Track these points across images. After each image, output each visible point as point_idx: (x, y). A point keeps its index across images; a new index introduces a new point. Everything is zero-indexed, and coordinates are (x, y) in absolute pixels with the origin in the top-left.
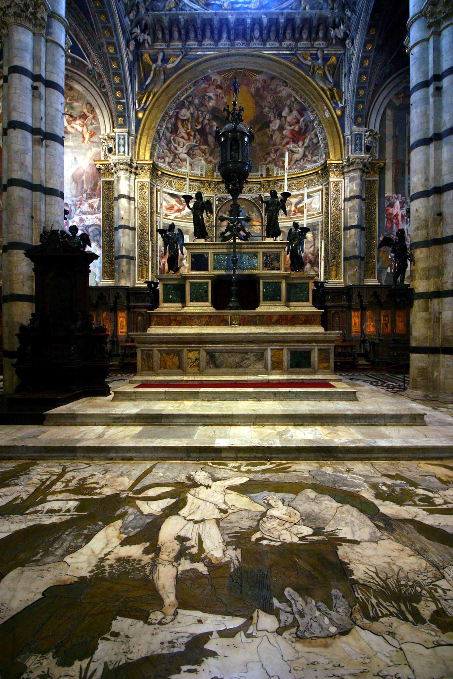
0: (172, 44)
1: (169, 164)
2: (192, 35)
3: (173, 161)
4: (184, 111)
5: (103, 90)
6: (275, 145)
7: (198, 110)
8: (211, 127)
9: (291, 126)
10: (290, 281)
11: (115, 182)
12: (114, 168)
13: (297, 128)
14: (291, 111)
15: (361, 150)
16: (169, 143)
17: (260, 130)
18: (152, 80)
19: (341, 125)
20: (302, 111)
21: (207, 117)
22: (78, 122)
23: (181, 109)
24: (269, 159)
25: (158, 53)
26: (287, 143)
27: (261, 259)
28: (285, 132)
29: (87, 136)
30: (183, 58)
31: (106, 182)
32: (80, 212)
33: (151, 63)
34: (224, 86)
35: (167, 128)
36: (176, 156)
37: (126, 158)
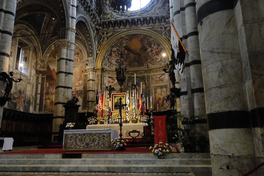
0: (109, 28)
1: (108, 66)
3: (110, 65)
4: (114, 48)
5: (85, 45)
8: (125, 52)
9: (155, 50)
11: (88, 75)
12: (88, 70)
14: (155, 45)
16: (108, 59)
17: (143, 52)
18: (102, 40)
20: (159, 45)
21: (123, 49)
22: (76, 56)
23: (113, 48)
24: (148, 62)
25: (104, 32)
28: (153, 52)
29: (79, 60)
30: (113, 32)
31: (85, 75)
32: (75, 86)
33: (102, 35)
35: (108, 55)
36: (111, 63)
37: (92, 67)
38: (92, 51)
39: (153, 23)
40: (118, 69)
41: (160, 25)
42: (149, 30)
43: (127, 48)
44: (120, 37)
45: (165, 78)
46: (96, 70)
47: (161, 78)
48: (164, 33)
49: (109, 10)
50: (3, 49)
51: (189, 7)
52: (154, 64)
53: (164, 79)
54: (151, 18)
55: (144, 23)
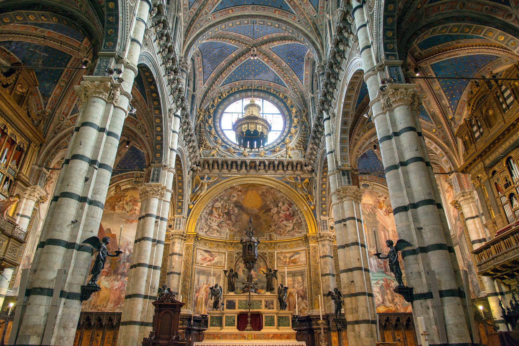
1: (206, 232)
2: (225, 167)
4: (217, 203)
6: (274, 221)
7: (226, 202)
8: (234, 211)
10: (280, 315)
12: (171, 237)
13: (288, 213)
14: (284, 204)
15: (327, 229)
19: (314, 214)
20: (290, 205)
21: (232, 205)
25: (204, 176)
26: (282, 221)
27: (263, 303)
28: (280, 215)
34: (243, 191)
35: (206, 213)
36: (210, 227)
38: (182, 205)
39: (283, 169)
40: (245, 242)
41: (294, 174)
42: (277, 180)
43: (237, 205)
44: (228, 187)
45: (301, 259)
46: (186, 237)
47: (293, 258)
48: (300, 186)
49: (214, 143)
50: (98, 195)
51: (416, 162)
52: (282, 234)
53: (298, 260)
54: (281, 163)
55: (269, 168)
